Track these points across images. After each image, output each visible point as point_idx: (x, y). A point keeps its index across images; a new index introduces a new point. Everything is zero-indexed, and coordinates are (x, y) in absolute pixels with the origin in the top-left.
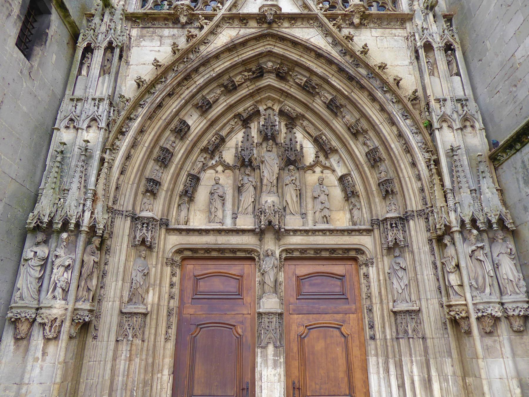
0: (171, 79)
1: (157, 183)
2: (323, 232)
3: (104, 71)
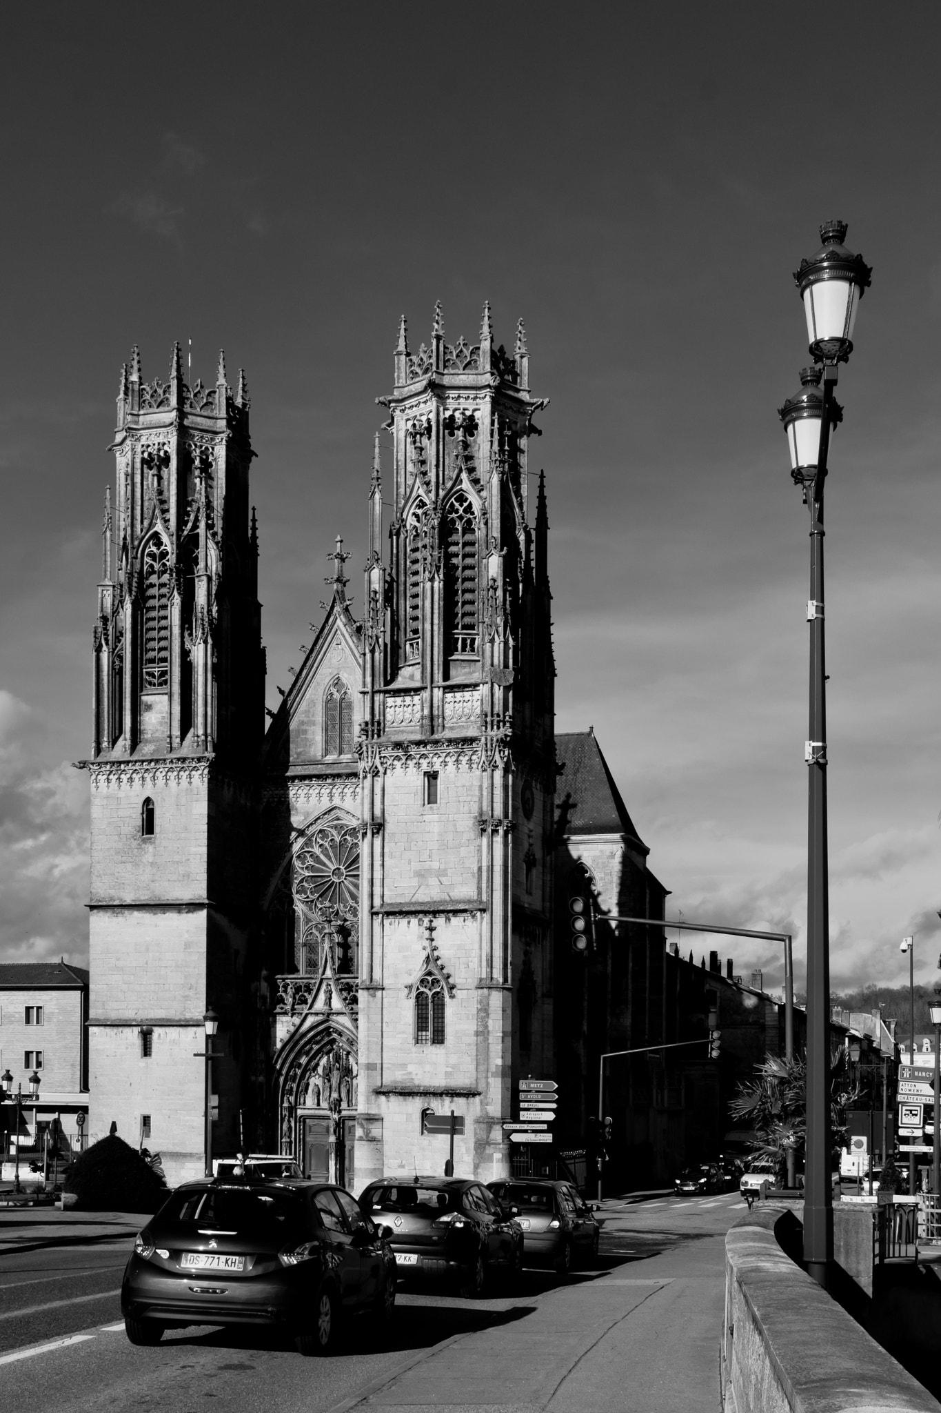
0: (288, 1048)
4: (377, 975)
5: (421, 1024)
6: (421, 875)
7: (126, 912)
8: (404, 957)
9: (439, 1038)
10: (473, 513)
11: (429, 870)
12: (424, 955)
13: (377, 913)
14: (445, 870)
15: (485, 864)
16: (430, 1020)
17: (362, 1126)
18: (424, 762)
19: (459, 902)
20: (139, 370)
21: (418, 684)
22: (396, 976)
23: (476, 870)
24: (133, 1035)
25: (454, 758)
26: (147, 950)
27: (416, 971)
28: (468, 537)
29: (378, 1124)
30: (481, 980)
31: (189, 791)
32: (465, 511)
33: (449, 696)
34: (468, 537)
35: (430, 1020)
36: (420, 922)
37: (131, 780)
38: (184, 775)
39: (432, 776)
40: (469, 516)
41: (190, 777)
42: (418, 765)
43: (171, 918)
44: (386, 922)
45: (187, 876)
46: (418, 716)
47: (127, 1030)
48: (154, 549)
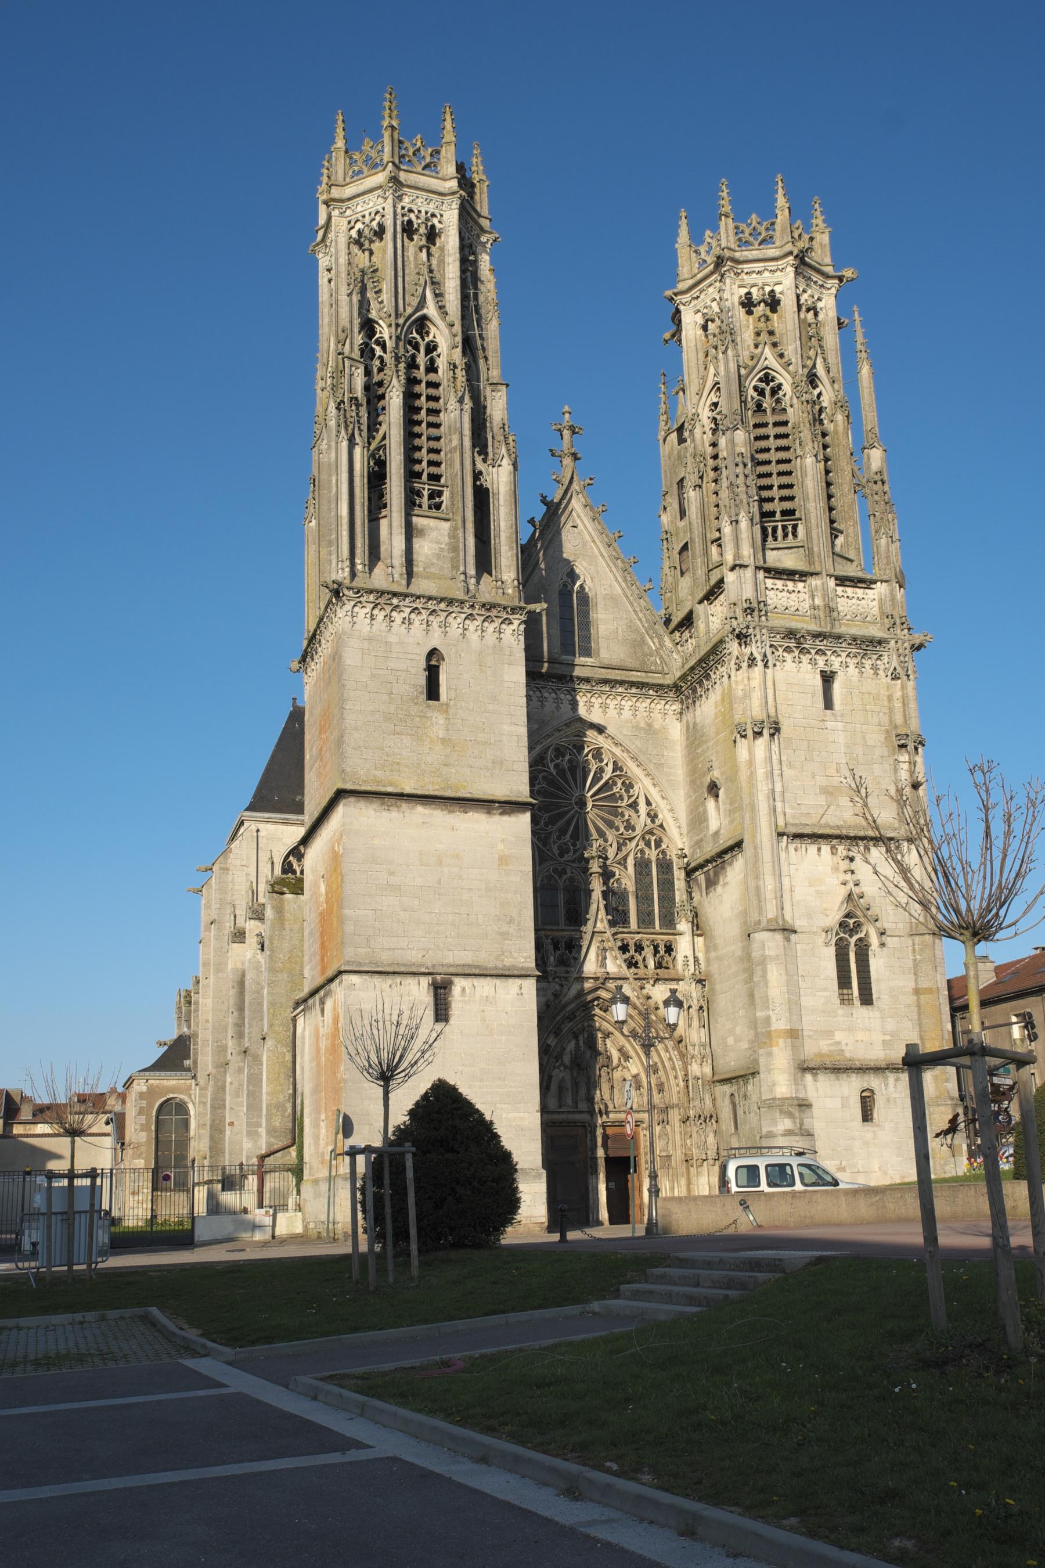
5: (844, 982)
7: (404, 805)
8: (817, 892)
9: (867, 998)
12: (843, 892)
13: (780, 835)
17: (790, 1115)
18: (821, 660)
26: (440, 863)
33: (840, 589)
36: (834, 851)
37: (407, 622)
38: (490, 627)
39: (828, 678)
42: (813, 662)
43: (476, 821)
44: (792, 847)
46: (806, 605)
47: (411, 981)
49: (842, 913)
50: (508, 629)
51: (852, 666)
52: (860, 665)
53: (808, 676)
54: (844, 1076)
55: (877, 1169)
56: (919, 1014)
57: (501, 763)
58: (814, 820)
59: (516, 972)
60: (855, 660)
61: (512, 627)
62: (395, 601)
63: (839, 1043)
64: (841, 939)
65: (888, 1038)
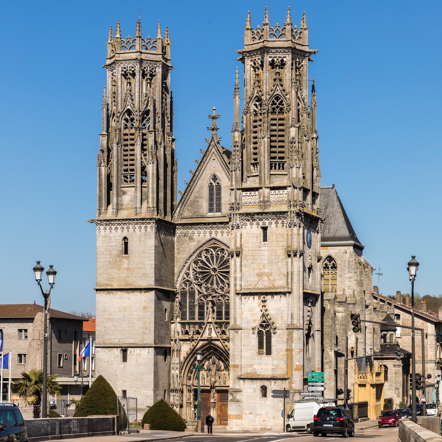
1: (190, 377)
2: (224, 387)
3: (177, 356)
4: (238, 323)
5: (260, 346)
6: (260, 275)
8: (252, 314)
9: (269, 352)
10: (283, 105)
11: (264, 273)
12: (261, 314)
13: (238, 294)
14: (271, 273)
15: (290, 270)
16: (265, 343)
17: (232, 394)
18: (261, 223)
19: (279, 288)
20: (120, 31)
21: (257, 186)
22: (248, 323)
23: (286, 273)
24: (118, 352)
25: (275, 221)
26: (125, 310)
27: (257, 320)
28: (281, 116)
29: (239, 393)
30: (289, 325)
31: (146, 234)
32: (279, 104)
33: (273, 192)
34: (281, 116)
35: (265, 343)
37: (116, 229)
39: (265, 229)
40: (281, 106)
41: (146, 228)
42: (258, 224)
43: (137, 295)
45: (144, 275)
48: (127, 116)
49: (260, 321)
50: (149, 226)
51: (273, 223)
52: (277, 223)
53: (255, 230)
54: (255, 381)
55: (264, 414)
56: (287, 358)
57: (145, 274)
58: (253, 287)
59: (147, 346)
60: (275, 221)
61: (151, 225)
62: (112, 222)
63: (255, 369)
64: (261, 331)
65: (274, 367)
